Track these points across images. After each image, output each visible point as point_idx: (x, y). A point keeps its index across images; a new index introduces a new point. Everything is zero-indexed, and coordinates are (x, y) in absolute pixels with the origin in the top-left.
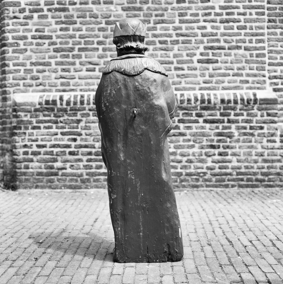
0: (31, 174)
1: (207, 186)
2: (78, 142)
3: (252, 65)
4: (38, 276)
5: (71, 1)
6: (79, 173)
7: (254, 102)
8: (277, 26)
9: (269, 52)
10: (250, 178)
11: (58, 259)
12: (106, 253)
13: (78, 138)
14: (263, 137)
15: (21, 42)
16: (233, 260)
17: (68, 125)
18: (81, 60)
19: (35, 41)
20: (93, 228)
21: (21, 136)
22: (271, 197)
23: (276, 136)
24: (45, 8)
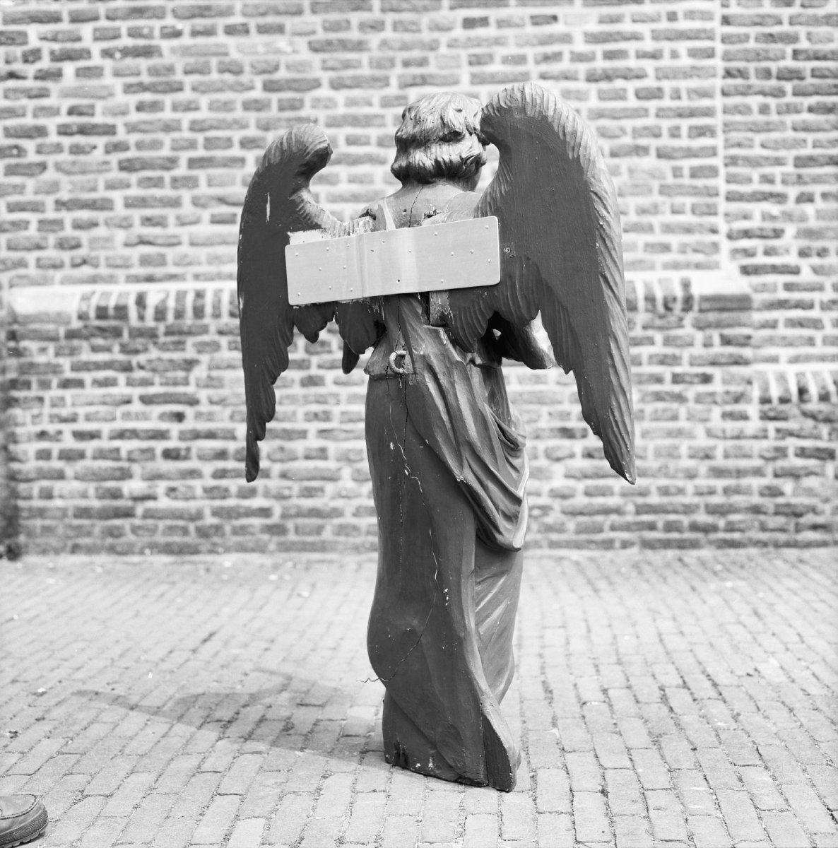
0: (59, 514)
1: (553, 545)
2: (189, 424)
3: (678, 200)
4: (7, 774)
5: (166, 27)
6: (193, 511)
7: (686, 307)
8: (749, 87)
9: (728, 161)
10: (675, 522)
11: (70, 735)
12: (202, 721)
13: (189, 411)
14: (710, 403)
15: (29, 145)
16: (532, 737)
17: (161, 376)
18: (196, 192)
19: (67, 141)
20: (192, 657)
21: (30, 408)
22: (725, 575)
23: (749, 401)
24: (96, 48)
